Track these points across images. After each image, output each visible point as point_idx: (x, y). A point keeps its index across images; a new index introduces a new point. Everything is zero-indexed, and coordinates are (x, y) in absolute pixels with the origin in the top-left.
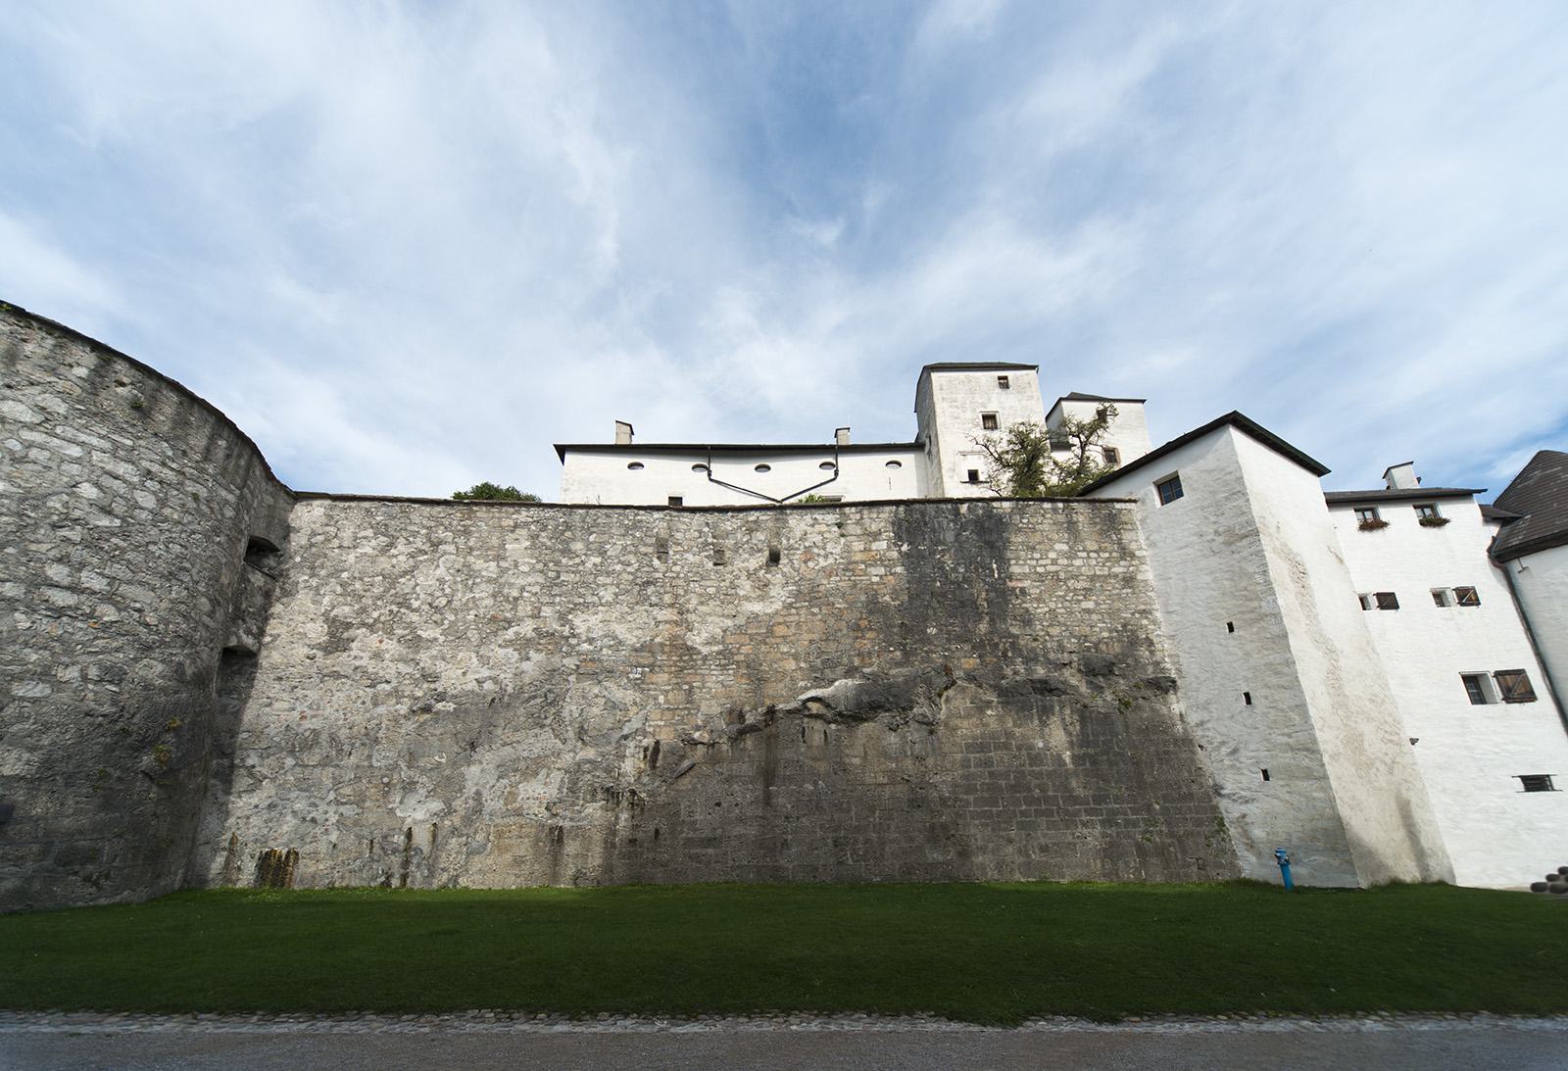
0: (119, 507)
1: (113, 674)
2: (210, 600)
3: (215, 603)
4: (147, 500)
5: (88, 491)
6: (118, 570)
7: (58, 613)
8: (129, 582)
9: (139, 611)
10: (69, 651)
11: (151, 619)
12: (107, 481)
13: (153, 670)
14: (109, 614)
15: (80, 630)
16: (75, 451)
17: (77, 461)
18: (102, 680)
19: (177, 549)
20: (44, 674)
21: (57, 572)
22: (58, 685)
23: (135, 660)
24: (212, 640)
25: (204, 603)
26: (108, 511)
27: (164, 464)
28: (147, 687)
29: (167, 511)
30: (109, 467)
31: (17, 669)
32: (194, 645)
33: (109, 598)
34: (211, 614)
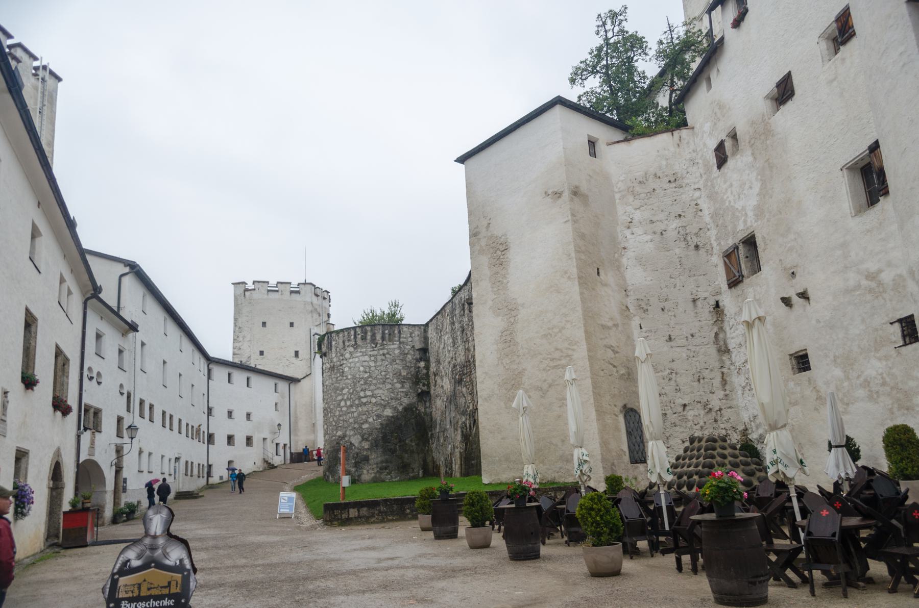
0: (367, 370)
1: (379, 416)
2: (400, 383)
3: (402, 383)
4: (372, 364)
5: (362, 369)
6: (372, 387)
7: (365, 404)
8: (375, 390)
10: (369, 414)
13: (388, 412)
14: (374, 400)
15: (369, 407)
16: (357, 360)
17: (358, 362)
19: (383, 373)
20: (366, 422)
21: (362, 394)
22: (369, 423)
23: (383, 411)
24: (407, 395)
25: (398, 385)
26: (366, 372)
28: (387, 416)
29: (378, 364)
30: (363, 360)
31: (362, 421)
32: (399, 400)
33: (372, 396)
34: (403, 387)
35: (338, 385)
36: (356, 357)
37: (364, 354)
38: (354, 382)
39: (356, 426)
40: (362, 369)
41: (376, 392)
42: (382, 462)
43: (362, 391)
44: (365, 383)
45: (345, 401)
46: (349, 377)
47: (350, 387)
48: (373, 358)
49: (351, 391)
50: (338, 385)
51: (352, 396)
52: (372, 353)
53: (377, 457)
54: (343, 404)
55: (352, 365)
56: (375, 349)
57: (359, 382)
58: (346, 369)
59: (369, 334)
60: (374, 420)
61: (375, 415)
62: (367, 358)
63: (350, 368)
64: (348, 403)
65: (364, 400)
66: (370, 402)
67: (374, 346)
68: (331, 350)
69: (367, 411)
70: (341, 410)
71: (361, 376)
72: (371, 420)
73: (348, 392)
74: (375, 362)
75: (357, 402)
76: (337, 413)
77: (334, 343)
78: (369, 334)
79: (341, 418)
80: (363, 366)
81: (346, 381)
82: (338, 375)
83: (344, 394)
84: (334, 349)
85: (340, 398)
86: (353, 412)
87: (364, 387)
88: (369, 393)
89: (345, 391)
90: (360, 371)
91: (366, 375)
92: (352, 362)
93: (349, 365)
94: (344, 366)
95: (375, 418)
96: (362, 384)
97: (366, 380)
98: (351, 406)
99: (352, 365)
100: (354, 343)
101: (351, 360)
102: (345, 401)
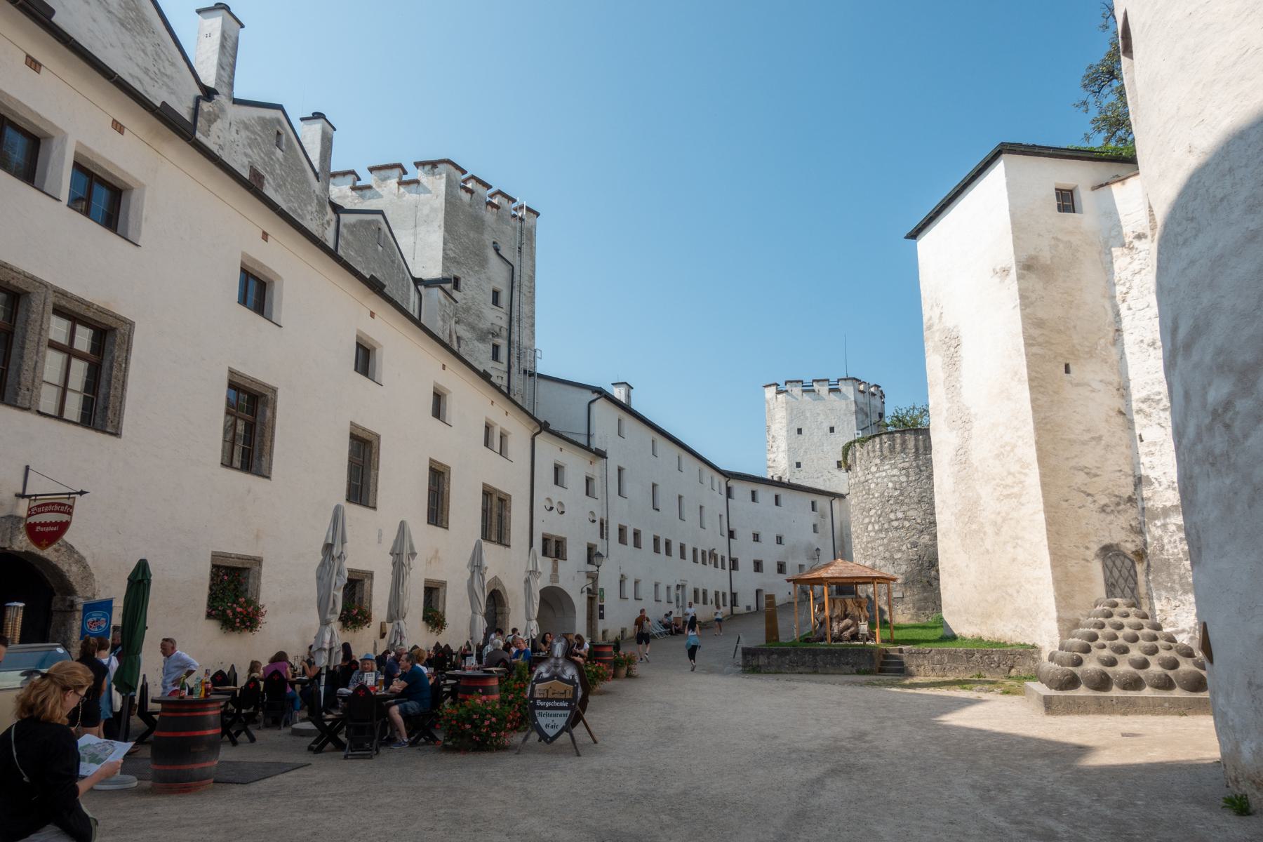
0: (898, 487)
1: (915, 545)
4: (903, 479)
5: (890, 485)
6: (905, 508)
7: (896, 529)
8: (909, 510)
9: (914, 519)
11: (919, 521)
12: (895, 478)
14: (907, 524)
16: (884, 474)
17: (885, 477)
18: (912, 548)
19: (918, 490)
20: (899, 550)
21: (892, 516)
23: (919, 537)
26: (896, 489)
27: (904, 462)
29: (910, 479)
33: (905, 519)
35: (864, 505)
36: (884, 471)
37: (894, 466)
38: (882, 502)
39: (887, 555)
40: (890, 485)
41: (908, 513)
42: (920, 600)
43: (891, 512)
44: (896, 503)
45: (873, 524)
46: (876, 495)
47: (878, 508)
48: (903, 472)
49: (879, 512)
50: (864, 505)
51: (881, 519)
52: (902, 465)
53: (914, 595)
54: (870, 528)
55: (879, 480)
56: (907, 460)
57: (888, 501)
58: (873, 486)
59: (898, 441)
60: (907, 547)
61: (910, 542)
62: (895, 472)
63: (877, 484)
64: (877, 527)
65: (895, 524)
66: (903, 527)
67: (905, 456)
68: (855, 462)
69: (899, 537)
70: (869, 535)
71: (890, 494)
72: (904, 548)
73: (876, 513)
74: (908, 476)
75: (886, 526)
76: (865, 540)
77: (858, 454)
78: (898, 441)
79: (870, 545)
80: (891, 481)
81: (873, 500)
82: (864, 493)
83: (872, 516)
84: (858, 462)
85: (867, 520)
86: (883, 539)
87: (894, 507)
88: (900, 515)
89: (872, 512)
90: (888, 488)
91: (897, 493)
92: (879, 477)
93: (875, 480)
94: (870, 481)
95: (909, 546)
96: (891, 504)
97: (896, 498)
98: (880, 531)
99: (879, 480)
100: (880, 453)
101: (877, 475)
102: (873, 524)
